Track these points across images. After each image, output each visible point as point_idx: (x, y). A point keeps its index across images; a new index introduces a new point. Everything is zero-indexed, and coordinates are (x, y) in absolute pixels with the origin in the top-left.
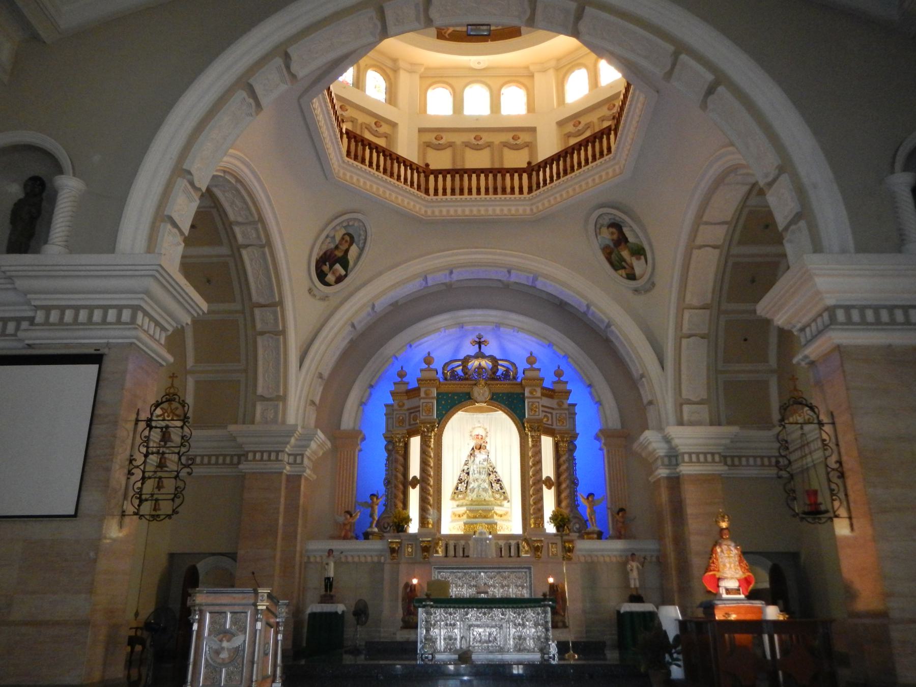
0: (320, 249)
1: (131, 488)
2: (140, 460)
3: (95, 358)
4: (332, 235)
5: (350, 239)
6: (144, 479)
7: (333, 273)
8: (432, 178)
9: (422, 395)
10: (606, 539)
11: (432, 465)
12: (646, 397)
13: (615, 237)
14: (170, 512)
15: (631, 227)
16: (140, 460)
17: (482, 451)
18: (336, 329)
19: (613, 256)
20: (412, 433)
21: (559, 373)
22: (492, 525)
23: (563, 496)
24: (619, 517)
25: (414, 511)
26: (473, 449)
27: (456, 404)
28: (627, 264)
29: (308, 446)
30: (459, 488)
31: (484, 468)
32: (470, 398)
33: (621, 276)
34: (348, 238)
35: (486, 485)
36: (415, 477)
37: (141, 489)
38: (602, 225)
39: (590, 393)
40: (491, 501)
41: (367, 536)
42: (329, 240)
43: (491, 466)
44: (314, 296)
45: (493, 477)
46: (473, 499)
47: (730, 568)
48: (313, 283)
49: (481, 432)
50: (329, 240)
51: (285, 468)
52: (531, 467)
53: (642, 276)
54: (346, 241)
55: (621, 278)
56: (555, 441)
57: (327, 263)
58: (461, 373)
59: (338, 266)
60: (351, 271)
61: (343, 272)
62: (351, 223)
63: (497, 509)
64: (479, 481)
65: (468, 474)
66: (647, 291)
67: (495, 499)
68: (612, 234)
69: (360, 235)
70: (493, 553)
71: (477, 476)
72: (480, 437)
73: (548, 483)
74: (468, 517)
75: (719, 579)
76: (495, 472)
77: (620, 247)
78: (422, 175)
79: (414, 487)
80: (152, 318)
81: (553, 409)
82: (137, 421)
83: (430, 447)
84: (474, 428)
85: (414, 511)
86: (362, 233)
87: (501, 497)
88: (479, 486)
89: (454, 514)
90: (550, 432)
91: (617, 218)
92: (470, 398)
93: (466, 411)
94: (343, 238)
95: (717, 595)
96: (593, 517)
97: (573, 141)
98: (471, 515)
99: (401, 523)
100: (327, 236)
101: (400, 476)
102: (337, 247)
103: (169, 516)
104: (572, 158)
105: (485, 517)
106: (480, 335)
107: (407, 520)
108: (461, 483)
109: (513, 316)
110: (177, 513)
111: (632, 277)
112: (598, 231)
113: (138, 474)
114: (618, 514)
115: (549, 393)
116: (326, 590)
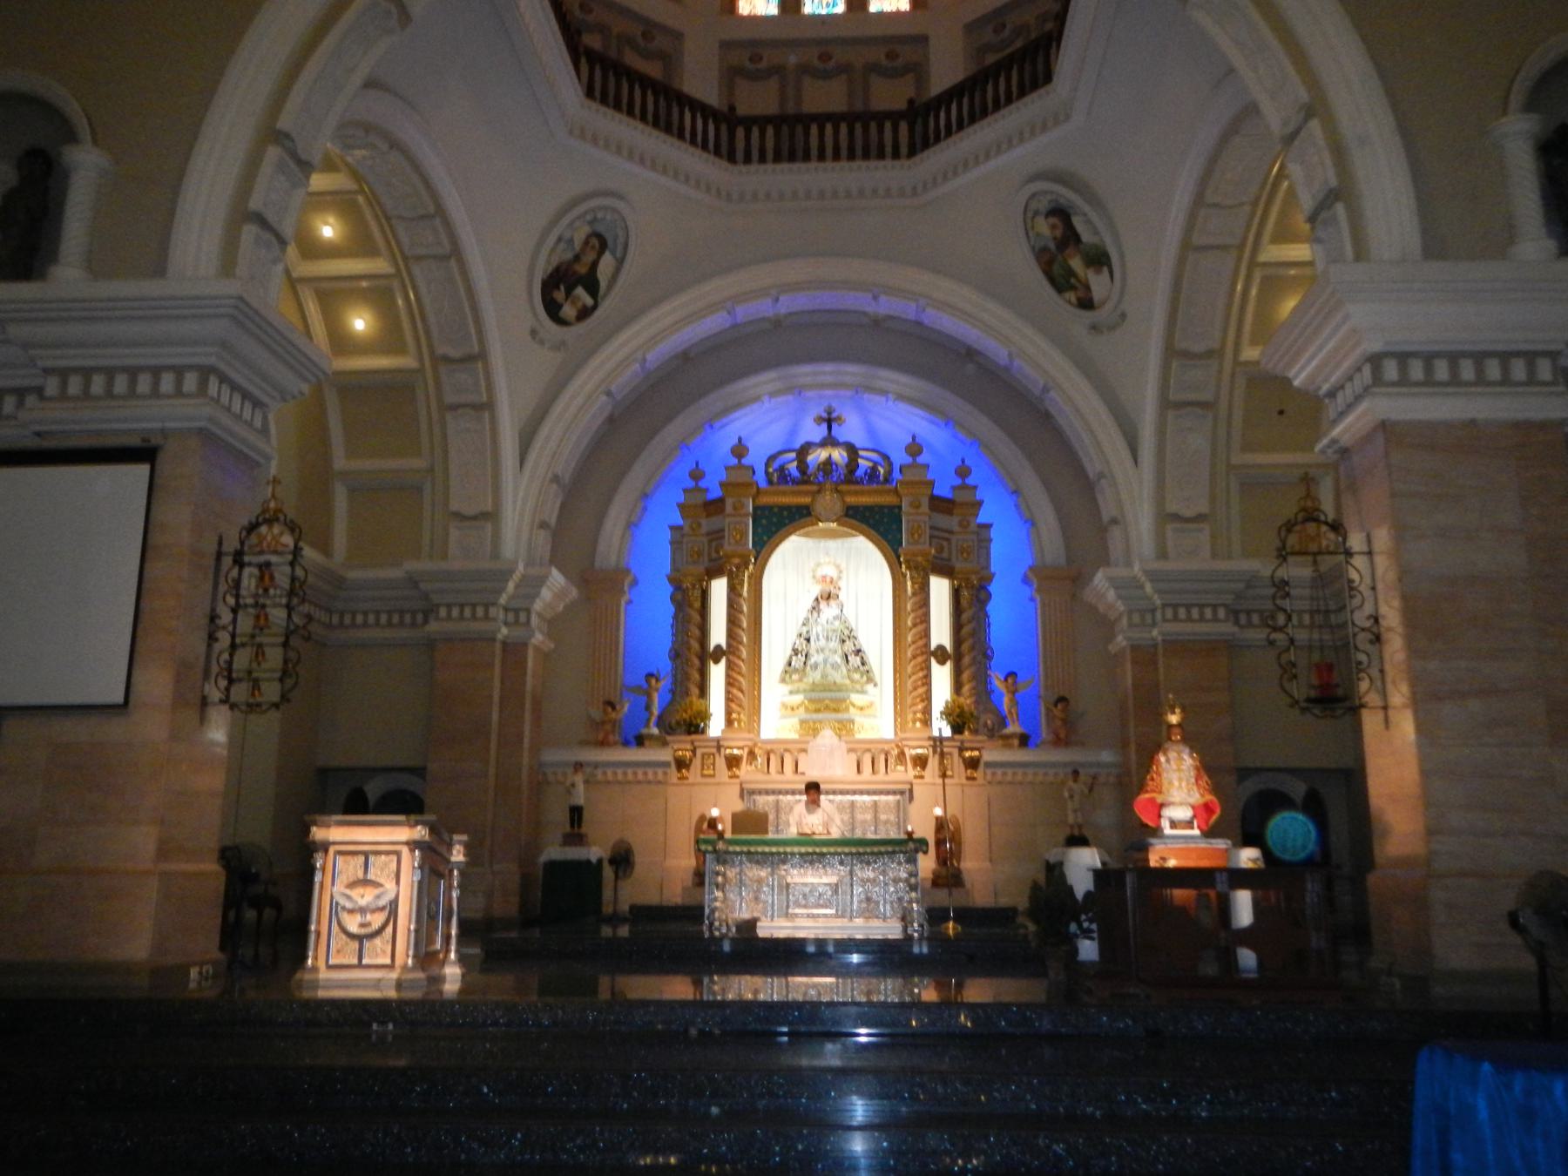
0: (548, 262)
1: (214, 662)
2: (226, 617)
3: (144, 453)
4: (567, 235)
5: (600, 242)
6: (233, 647)
7: (573, 303)
8: (740, 133)
9: (729, 508)
10: (1037, 746)
11: (745, 625)
12: (1107, 511)
13: (1058, 233)
14: (276, 699)
15: (1085, 215)
16: (226, 617)
17: (832, 602)
18: (580, 400)
19: (1056, 269)
20: (714, 573)
21: (963, 472)
23: (965, 676)
24: (1057, 712)
26: (817, 599)
27: (785, 525)
28: (1079, 281)
29: (537, 594)
30: (793, 664)
31: (834, 631)
32: (809, 514)
33: (1070, 302)
34: (595, 242)
35: (838, 659)
36: (718, 647)
37: (230, 663)
38: (1036, 213)
39: (1017, 506)
40: (846, 685)
41: (640, 741)
42: (562, 245)
43: (848, 628)
44: (542, 342)
45: (849, 646)
46: (816, 681)
47: (1180, 786)
48: (538, 320)
49: (831, 572)
50: (562, 245)
51: (499, 630)
52: (911, 629)
53: (1103, 303)
54: (593, 247)
55: (1069, 307)
56: (953, 585)
57: (562, 288)
58: (795, 473)
59: (580, 291)
60: (605, 295)
61: (589, 301)
62: (600, 215)
64: (826, 653)
65: (808, 640)
66: (1112, 328)
67: (852, 681)
68: (1053, 227)
69: (616, 238)
71: (822, 642)
72: (828, 580)
73: (941, 655)
74: (807, 710)
75: (1162, 806)
76: (853, 637)
77: (1067, 251)
78: (724, 128)
79: (717, 661)
80: (235, 387)
81: (951, 532)
82: (219, 555)
83: (741, 595)
84: (819, 565)
86: (621, 233)
87: (862, 677)
88: (825, 661)
89: (785, 706)
90: (945, 571)
91: (1062, 201)
92: (809, 514)
93: (807, 535)
94: (586, 242)
95: (1156, 832)
96: (1013, 711)
97: (991, 59)
98: (812, 707)
99: (694, 725)
100: (560, 239)
101: (695, 645)
102: (577, 258)
103: (276, 706)
104: (984, 91)
105: (836, 710)
106: (830, 407)
107: (705, 716)
108: (796, 654)
109: (884, 373)
110: (288, 700)
111: (1086, 304)
112: (1029, 221)
113: (224, 639)
114: (1056, 705)
115: (941, 505)
116: (572, 825)
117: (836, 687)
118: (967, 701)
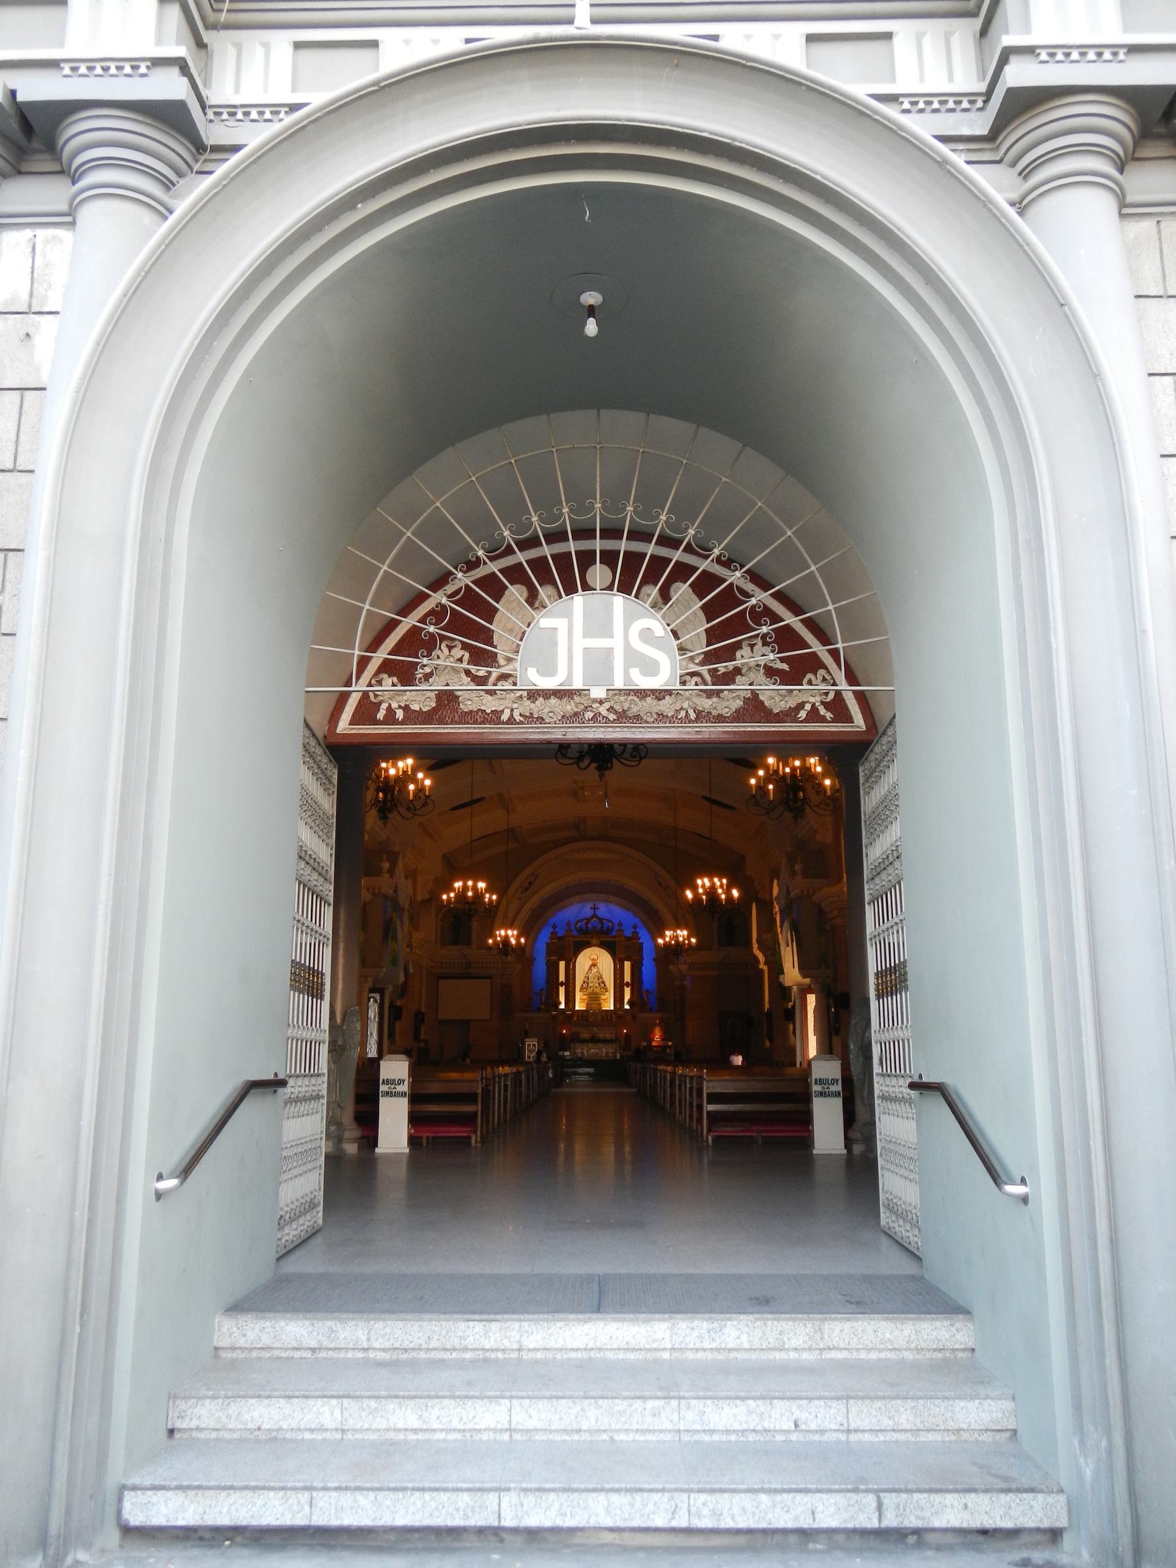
3: (489, 977)
22: (600, 1005)
25: (562, 998)
41: (539, 1010)
63: (603, 997)
64: (594, 983)
70: (599, 1018)
73: (627, 984)
85: (562, 998)
107: (560, 1003)
115: (628, 939)
117: (596, 994)
118: (635, 999)
